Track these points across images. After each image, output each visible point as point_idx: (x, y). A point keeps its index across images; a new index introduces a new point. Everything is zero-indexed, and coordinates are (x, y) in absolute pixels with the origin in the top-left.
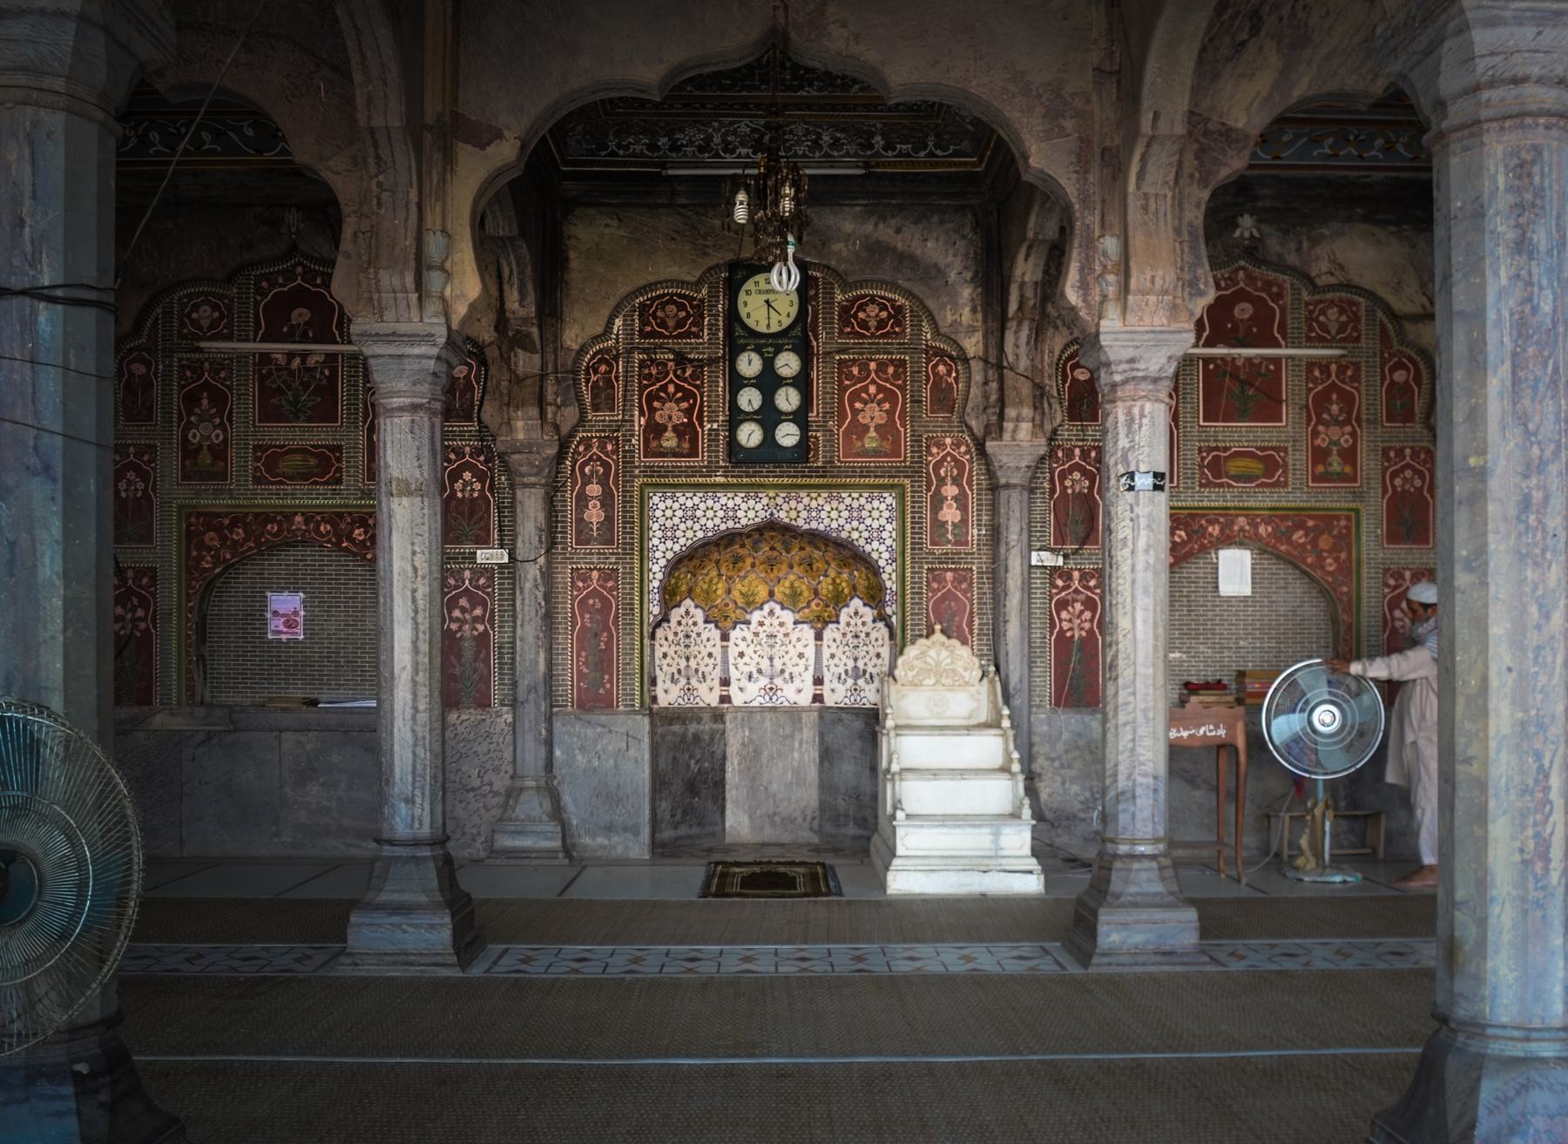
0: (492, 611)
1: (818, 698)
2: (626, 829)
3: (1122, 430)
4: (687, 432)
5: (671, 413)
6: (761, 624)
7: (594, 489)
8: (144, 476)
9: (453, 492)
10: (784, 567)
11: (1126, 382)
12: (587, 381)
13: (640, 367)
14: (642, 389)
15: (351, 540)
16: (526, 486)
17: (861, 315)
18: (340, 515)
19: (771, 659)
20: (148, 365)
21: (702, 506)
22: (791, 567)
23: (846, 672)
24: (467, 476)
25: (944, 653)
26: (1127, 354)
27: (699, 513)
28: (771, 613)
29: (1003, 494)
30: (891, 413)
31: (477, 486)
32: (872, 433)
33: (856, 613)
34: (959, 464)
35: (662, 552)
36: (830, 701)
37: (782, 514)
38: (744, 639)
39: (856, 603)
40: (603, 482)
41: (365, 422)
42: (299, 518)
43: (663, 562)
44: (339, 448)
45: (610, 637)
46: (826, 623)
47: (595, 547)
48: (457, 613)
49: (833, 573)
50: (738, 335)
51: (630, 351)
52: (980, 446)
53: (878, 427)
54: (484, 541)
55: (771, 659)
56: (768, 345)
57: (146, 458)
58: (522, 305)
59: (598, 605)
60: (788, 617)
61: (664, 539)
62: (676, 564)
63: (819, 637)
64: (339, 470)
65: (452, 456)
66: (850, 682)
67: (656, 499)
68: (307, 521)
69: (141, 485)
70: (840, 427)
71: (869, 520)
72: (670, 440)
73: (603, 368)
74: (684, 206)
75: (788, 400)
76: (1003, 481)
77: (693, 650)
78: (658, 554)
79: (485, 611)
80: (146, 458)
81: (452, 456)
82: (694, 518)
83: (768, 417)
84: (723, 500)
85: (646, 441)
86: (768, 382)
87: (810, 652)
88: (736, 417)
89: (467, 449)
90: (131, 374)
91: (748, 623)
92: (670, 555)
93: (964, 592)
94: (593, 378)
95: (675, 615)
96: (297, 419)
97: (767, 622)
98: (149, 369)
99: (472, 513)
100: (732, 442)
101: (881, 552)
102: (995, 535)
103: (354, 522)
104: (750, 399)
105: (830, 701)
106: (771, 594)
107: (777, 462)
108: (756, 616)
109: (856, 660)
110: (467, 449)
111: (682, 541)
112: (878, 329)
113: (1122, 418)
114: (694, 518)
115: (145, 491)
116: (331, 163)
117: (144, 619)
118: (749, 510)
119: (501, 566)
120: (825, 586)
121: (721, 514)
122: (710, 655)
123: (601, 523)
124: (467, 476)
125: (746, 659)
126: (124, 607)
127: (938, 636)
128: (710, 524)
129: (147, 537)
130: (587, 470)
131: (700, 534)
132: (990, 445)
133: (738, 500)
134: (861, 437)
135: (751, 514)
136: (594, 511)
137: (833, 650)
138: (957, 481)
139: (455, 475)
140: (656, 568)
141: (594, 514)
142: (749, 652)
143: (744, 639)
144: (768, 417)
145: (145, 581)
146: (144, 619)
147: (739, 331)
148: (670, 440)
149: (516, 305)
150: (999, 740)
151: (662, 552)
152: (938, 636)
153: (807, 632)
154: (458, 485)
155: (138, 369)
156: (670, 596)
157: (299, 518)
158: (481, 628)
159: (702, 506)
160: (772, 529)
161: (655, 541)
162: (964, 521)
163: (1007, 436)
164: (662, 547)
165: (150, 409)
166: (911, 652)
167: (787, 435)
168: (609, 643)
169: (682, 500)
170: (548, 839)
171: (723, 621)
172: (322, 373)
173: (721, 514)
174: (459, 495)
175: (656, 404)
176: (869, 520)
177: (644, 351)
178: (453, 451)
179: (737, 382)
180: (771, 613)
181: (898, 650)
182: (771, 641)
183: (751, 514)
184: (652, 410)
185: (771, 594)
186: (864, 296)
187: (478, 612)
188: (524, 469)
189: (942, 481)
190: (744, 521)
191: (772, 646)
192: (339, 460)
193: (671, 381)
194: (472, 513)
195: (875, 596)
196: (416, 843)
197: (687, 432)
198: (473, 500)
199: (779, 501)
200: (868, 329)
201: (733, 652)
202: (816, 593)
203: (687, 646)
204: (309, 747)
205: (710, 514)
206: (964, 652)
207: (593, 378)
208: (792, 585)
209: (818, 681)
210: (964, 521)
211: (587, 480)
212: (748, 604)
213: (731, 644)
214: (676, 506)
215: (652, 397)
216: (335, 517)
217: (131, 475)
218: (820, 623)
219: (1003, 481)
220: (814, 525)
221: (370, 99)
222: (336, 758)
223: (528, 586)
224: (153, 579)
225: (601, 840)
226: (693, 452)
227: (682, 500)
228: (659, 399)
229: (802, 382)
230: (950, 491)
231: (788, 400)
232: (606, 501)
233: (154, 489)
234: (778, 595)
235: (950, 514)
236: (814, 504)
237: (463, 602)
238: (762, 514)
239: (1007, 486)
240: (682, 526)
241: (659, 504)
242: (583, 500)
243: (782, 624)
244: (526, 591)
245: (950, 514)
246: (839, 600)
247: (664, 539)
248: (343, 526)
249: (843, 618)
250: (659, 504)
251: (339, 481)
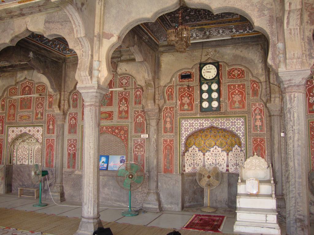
0: (145, 149)
1: (227, 170)
2: (175, 204)
3: (288, 102)
4: (190, 104)
5: (186, 100)
6: (213, 151)
7: (168, 119)
8: (75, 119)
9: (137, 121)
10: (219, 137)
11: (288, 87)
12: (167, 93)
13: (179, 89)
14: (179, 95)
15: (115, 132)
16: (151, 119)
17: (233, 73)
18: (113, 127)
19: (216, 160)
20: (77, 95)
21: (194, 123)
22: (220, 137)
23: (234, 164)
24: (140, 117)
25: (257, 161)
26: (288, 78)
27: (194, 125)
28: (216, 148)
29: (272, 117)
30: (242, 97)
31: (142, 119)
32: (237, 103)
33: (236, 149)
34: (261, 110)
36: (230, 171)
37: (215, 124)
38: (209, 155)
39: (236, 146)
40: (170, 118)
41: (118, 106)
42: (105, 128)
43: (185, 137)
44: (112, 112)
45: (172, 156)
46: (229, 151)
47: (168, 134)
48: (137, 150)
49: (229, 140)
50: (202, 80)
51: (176, 86)
52: (266, 105)
53: (238, 101)
54: (143, 132)
55: (216, 160)
56: (209, 82)
57: (76, 115)
58: (148, 77)
59: (169, 148)
60: (220, 149)
61: (185, 131)
63: (228, 155)
64: (113, 117)
65: (136, 113)
66: (235, 167)
67: (183, 121)
68: (106, 128)
69: (75, 121)
70: (229, 101)
72: (186, 107)
73: (170, 90)
74: (188, 51)
75: (215, 95)
76: (272, 114)
77: (195, 158)
78: (184, 135)
79: (143, 149)
80: (76, 115)
81: (136, 113)
82: (193, 126)
83: (210, 100)
84: (200, 121)
85: (180, 107)
86: (210, 91)
87: (226, 158)
88: (202, 100)
89: (140, 111)
90: (74, 98)
91: (210, 151)
92: (186, 135)
93: (263, 144)
94: (168, 93)
95: (190, 149)
96: (104, 106)
97: (215, 151)
98: (77, 97)
99: (140, 126)
100: (201, 106)
101: (240, 133)
102: (271, 129)
103: (116, 128)
104: (205, 96)
105: (230, 171)
106: (216, 144)
107: (212, 111)
108: (212, 149)
109: (236, 161)
110: (140, 111)
111: (190, 132)
112: (238, 76)
113: (288, 98)
114: (193, 126)
115: (75, 122)
116: (76, 48)
117: (74, 150)
118: (206, 124)
119: (147, 138)
120: (229, 142)
121: (199, 125)
122: (200, 159)
123: (170, 128)
124: (140, 117)
125: (209, 160)
126: (71, 147)
127: (256, 156)
128: (196, 127)
129: (75, 132)
130: (166, 115)
131: (194, 130)
132: (268, 104)
133: (203, 121)
134: (234, 104)
135: (207, 124)
136: (168, 125)
137: (231, 158)
138: (260, 114)
139: (137, 117)
140: (183, 138)
141: (168, 126)
142: (210, 158)
143: (209, 155)
144: (210, 100)
145: (75, 142)
146: (74, 150)
147: (202, 79)
148: (186, 107)
149: (147, 77)
150: (270, 187)
151: (185, 135)
152: (256, 156)
154: (138, 119)
155: (75, 97)
157: (105, 128)
158: (142, 153)
159: (194, 123)
160: (212, 128)
161: (183, 132)
162: (262, 125)
163: (272, 102)
164: (185, 133)
165: (77, 105)
166: (248, 160)
167: (215, 104)
168: (172, 157)
169: (189, 121)
170: (155, 206)
171: (204, 151)
172: (110, 95)
173: (199, 125)
174: (138, 122)
175: (183, 98)
176: (237, 126)
177: (180, 85)
178: (137, 111)
179: (202, 92)
180: (216, 148)
182: (216, 156)
183: (207, 124)
184: (182, 100)
185: (216, 144)
186: (234, 68)
187: (142, 149)
188: (151, 115)
189: (256, 115)
190: (205, 126)
191: (216, 157)
192: (113, 114)
193: (186, 92)
194: (140, 126)
195: (240, 145)
196: (89, 218)
197: (190, 104)
198: (141, 123)
199: (214, 121)
200: (235, 76)
201: (206, 158)
202: (227, 143)
203: (194, 157)
204: (105, 180)
205: (196, 125)
206: (263, 160)
207: (168, 93)
208: (221, 142)
209: (228, 166)
210: (262, 125)
211: (167, 117)
212: (210, 146)
213: (206, 156)
214: (188, 123)
215: (182, 96)
216: (112, 127)
217: (73, 119)
218: (228, 151)
219: (272, 114)
220: (223, 127)
221: (77, 31)
222: (111, 183)
223: (152, 143)
224: (76, 141)
225: (169, 206)
226: (192, 110)
227: (189, 121)
228: (183, 97)
231: (215, 95)
232: (171, 123)
233: (77, 122)
234: (217, 144)
235: (258, 123)
236: (223, 121)
237: (138, 147)
238: (209, 124)
239: (273, 115)
240: (190, 128)
242: (165, 122)
243: (218, 151)
244: (152, 144)
246: (232, 145)
247: (185, 131)
248: (113, 129)
249: (233, 150)
251: (112, 119)
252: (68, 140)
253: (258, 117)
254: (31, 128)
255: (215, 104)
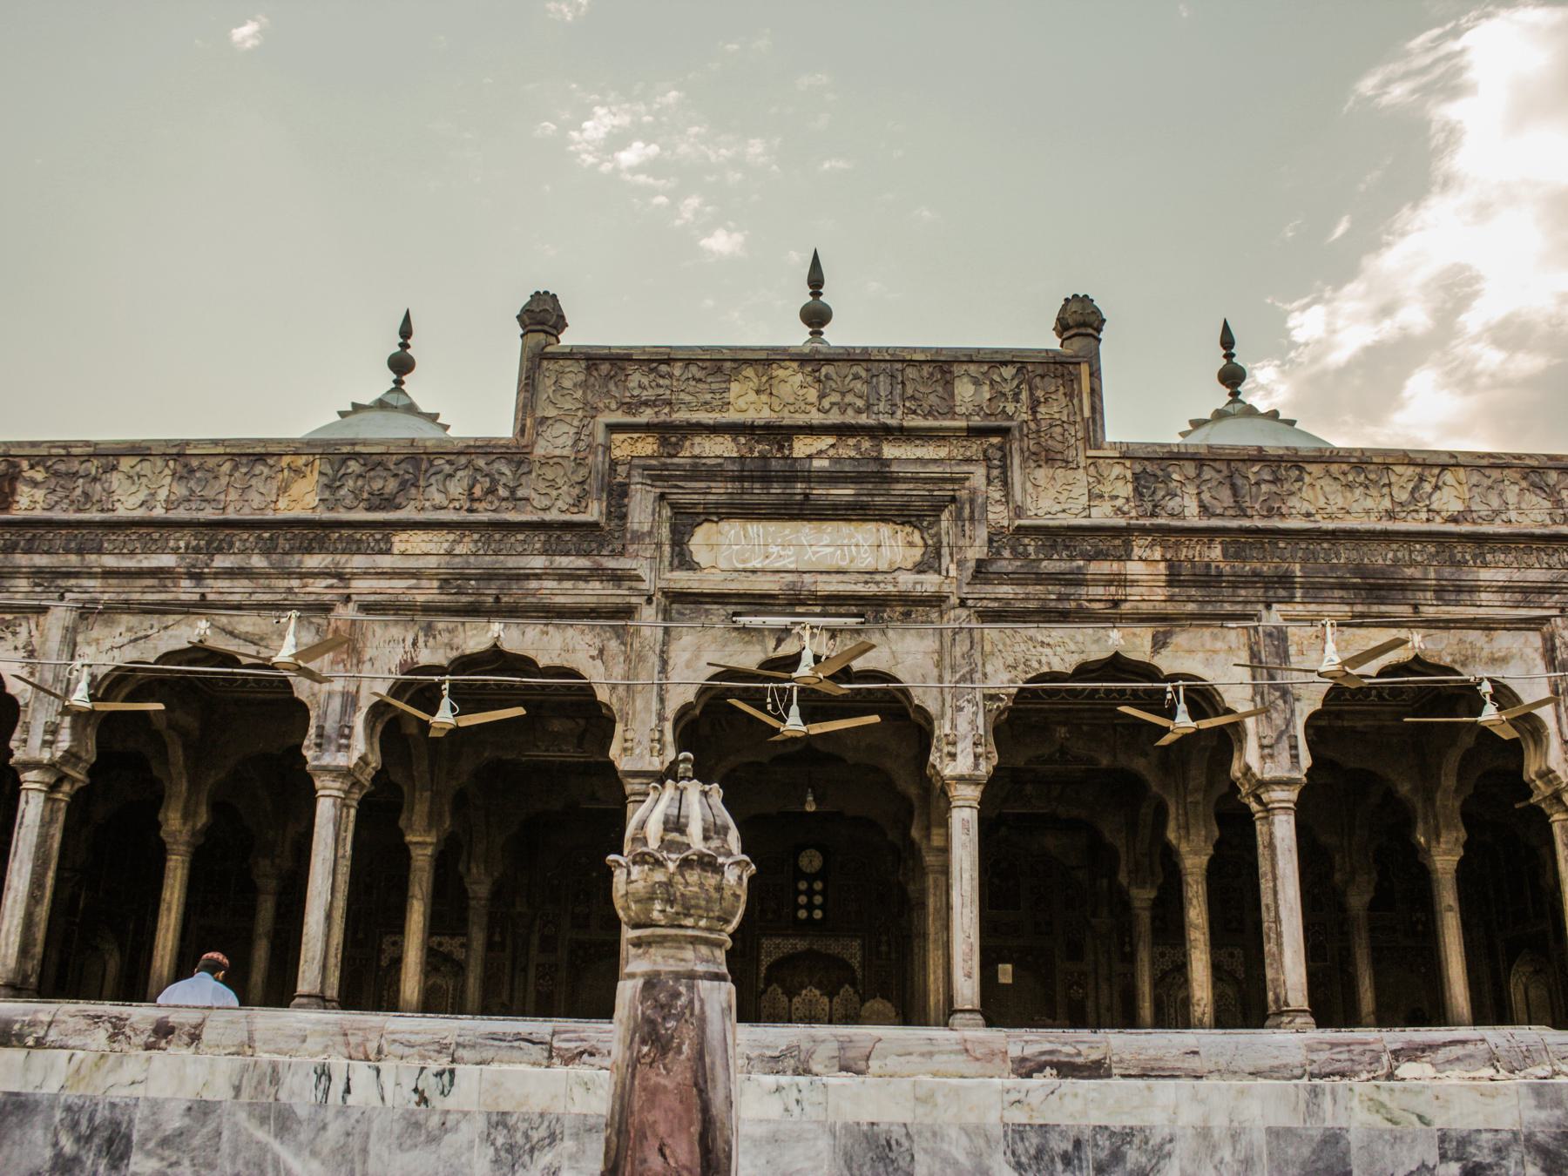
35: (766, 961)
50: (800, 874)
56: (811, 878)
60: (817, 992)
62: (769, 968)
71: (852, 951)
72: (770, 916)
75: (818, 900)
83: (810, 907)
86: (810, 893)
88: (798, 907)
100: (795, 917)
104: (803, 899)
118: (801, 945)
144: (810, 907)
148: (770, 916)
151: (766, 961)
153: (826, 1000)
156: (768, 981)
160: (809, 953)
166: (868, 1004)
176: (852, 951)
181: (863, 1001)
195: (853, 985)
218: (831, 995)
229: (823, 893)
230: (884, 938)
231: (818, 900)
235: (884, 948)
241: (765, 942)
245: (884, 948)
250: (765, 942)
252: (538, 965)
253: (884, 938)
254: (445, 939)
255: (818, 914)
